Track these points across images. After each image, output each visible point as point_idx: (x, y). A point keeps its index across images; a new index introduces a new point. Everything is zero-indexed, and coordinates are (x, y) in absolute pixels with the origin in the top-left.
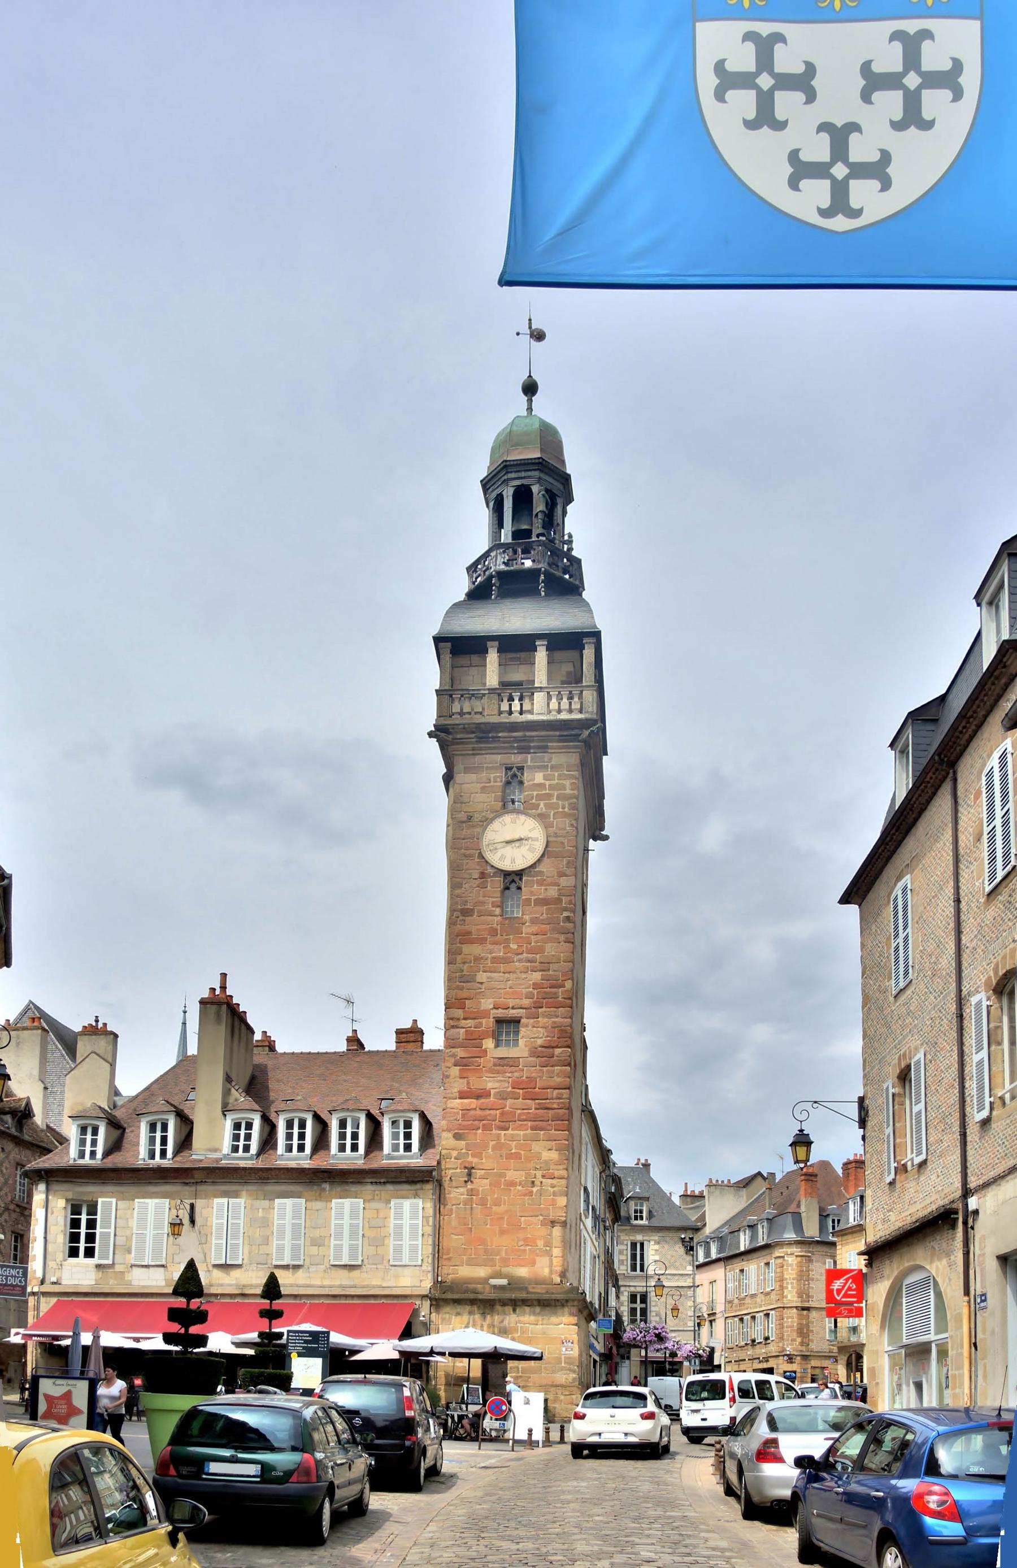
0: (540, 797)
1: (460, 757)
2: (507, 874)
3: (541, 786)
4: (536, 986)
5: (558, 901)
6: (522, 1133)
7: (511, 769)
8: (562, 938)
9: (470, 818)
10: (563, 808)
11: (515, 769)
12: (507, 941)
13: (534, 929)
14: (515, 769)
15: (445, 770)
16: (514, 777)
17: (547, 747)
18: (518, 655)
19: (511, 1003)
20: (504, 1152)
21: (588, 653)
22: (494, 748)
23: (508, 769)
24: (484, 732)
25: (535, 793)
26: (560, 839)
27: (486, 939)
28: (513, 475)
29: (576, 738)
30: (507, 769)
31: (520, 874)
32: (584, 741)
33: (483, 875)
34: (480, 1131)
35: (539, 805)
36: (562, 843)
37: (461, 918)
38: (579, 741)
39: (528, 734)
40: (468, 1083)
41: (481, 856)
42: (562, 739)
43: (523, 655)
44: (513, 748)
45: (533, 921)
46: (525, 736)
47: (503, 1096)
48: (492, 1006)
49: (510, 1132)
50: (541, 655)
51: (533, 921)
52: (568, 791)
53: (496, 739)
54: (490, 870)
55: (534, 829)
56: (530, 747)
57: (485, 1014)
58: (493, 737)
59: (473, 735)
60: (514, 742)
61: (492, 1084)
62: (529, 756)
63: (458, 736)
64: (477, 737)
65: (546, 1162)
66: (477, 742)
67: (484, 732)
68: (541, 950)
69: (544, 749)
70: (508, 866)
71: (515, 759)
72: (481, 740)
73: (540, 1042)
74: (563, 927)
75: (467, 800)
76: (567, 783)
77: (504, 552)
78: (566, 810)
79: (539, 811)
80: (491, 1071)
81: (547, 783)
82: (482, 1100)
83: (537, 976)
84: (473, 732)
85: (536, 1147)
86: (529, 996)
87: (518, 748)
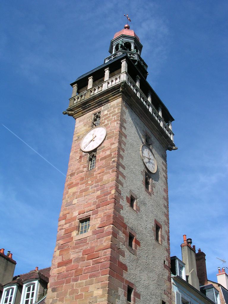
0: (105, 119)
2: (90, 152)
3: (107, 114)
4: (98, 197)
6: (84, 281)
11: (97, 114)
12: (88, 181)
14: (97, 114)
16: (97, 117)
17: (108, 101)
19: (86, 209)
20: (74, 295)
31: (95, 150)
32: (122, 92)
34: (65, 284)
40: (62, 257)
45: (99, 168)
47: (78, 260)
48: (77, 214)
49: (79, 281)
54: (84, 154)
56: (102, 104)
57: (74, 219)
59: (81, 108)
61: (73, 255)
65: (96, 297)
66: (83, 110)
68: (101, 180)
73: (97, 226)
76: (116, 110)
80: (74, 248)
81: (109, 113)
82: (69, 266)
83: (99, 193)
85: (91, 288)
86: (94, 203)
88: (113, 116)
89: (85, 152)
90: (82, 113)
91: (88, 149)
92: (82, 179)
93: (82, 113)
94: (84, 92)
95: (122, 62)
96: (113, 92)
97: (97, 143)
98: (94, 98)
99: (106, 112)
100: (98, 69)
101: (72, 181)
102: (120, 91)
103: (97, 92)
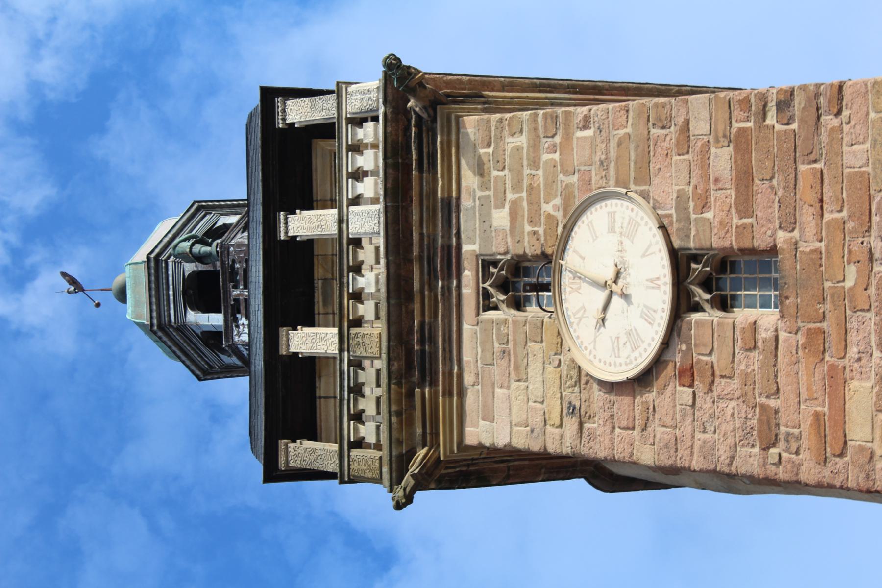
1: (469, 430)
2: (682, 304)
3: (514, 215)
5: (741, 143)
7: (487, 295)
8: (829, 121)
9: (573, 410)
10: (553, 149)
11: (485, 285)
12: (841, 296)
13: (807, 216)
14: (485, 285)
15: (583, 480)
18: (319, 284)
21: (297, 112)
22: (448, 340)
23: (487, 303)
24: (409, 367)
25: (528, 228)
26: (613, 144)
27: (832, 367)
28: (172, 312)
29: (427, 128)
30: (488, 307)
33: (687, 375)
35: (549, 216)
36: (619, 144)
37: (782, 444)
38: (434, 120)
39: (415, 252)
41: (643, 380)
42: (428, 162)
43: (319, 272)
44: (447, 289)
46: (421, 257)
50: (302, 224)
51: (790, 223)
52: (522, 140)
53: (428, 336)
55: (590, 225)
56: (447, 248)
58: (422, 342)
60: (433, 288)
62: (466, 248)
63: (419, 431)
64: (422, 385)
66: (434, 383)
67: (409, 367)
69: (450, 208)
70: (662, 299)
71: (469, 281)
72: (428, 376)
74: (802, 121)
75: (540, 419)
76: (512, 142)
77: (238, 326)
78: (557, 139)
79: (559, 215)
81: (510, 196)
84: (411, 395)
87: (448, 277)
88: (535, 164)
89: (666, 344)
90: (448, 393)
91: (657, 316)
92: (816, 344)
93: (448, 393)
94: (342, 373)
95: (284, 119)
96: (414, 157)
97: (644, 256)
98: (398, 288)
99: (501, 218)
100: (259, 175)
101: (806, 426)
102: (425, 115)
103: (374, 333)
